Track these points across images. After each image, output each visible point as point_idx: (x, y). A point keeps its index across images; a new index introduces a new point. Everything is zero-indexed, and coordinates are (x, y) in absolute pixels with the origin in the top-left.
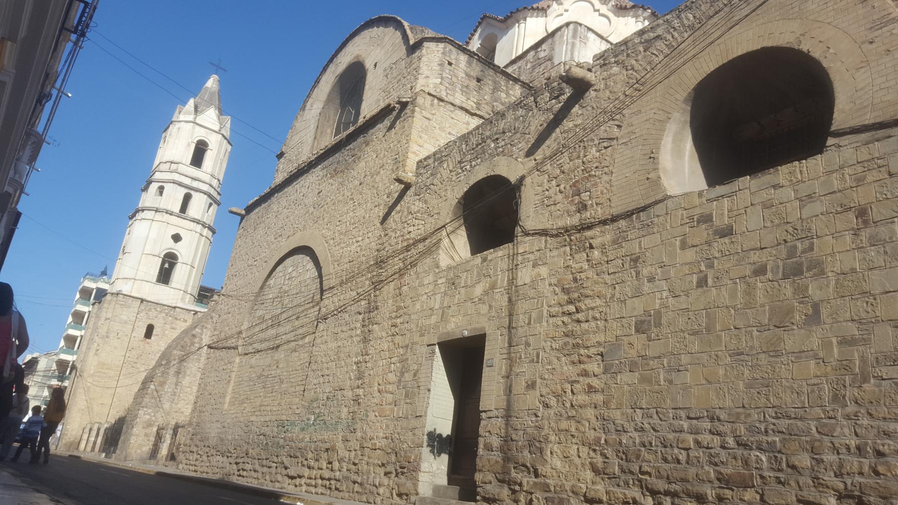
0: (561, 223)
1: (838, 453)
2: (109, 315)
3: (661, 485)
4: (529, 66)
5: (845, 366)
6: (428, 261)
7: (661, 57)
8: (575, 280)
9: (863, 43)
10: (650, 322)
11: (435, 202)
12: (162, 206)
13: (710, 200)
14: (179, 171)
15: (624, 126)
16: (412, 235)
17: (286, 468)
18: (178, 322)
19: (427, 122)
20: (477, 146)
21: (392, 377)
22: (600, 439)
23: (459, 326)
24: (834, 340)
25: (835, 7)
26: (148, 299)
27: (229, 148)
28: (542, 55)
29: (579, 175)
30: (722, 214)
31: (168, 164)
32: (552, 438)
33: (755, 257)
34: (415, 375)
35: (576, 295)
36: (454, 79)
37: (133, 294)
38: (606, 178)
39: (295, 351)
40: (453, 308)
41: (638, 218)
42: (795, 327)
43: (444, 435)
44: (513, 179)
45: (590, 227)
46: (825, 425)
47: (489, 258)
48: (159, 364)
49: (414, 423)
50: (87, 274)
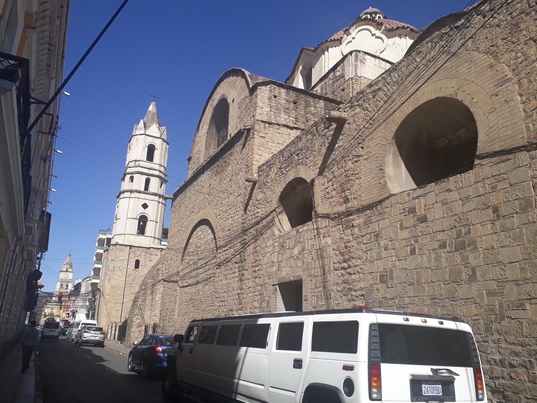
0: (336, 210)
1: (491, 365)
5: (491, 309)
6: (269, 232)
7: (382, 103)
8: (346, 247)
9: (492, 95)
10: (387, 276)
11: (269, 193)
12: (134, 188)
15: (365, 147)
16: (259, 214)
18: (153, 256)
19: (262, 140)
20: (288, 158)
21: (256, 304)
23: (287, 274)
24: (484, 292)
25: (476, 70)
27: (168, 147)
28: (338, 74)
29: (343, 179)
30: (421, 208)
31: (134, 162)
33: (440, 236)
34: (268, 304)
35: (347, 257)
38: (357, 181)
39: (206, 284)
40: (284, 262)
41: (377, 208)
42: (463, 283)
44: (308, 181)
45: (351, 214)
46: (482, 346)
47: (300, 231)
48: (141, 289)
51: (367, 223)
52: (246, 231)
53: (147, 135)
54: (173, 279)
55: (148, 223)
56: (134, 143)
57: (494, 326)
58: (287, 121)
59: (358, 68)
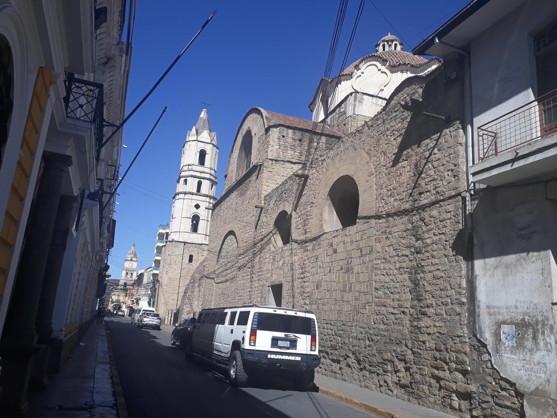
2: (170, 253)
6: (268, 247)
11: (269, 218)
12: (188, 190)
13: (334, 237)
14: (193, 169)
19: (270, 174)
21: (259, 299)
23: (275, 279)
27: (218, 151)
28: (342, 110)
29: (304, 217)
36: (286, 144)
38: (311, 220)
39: (232, 283)
40: (274, 270)
45: (306, 243)
51: (313, 249)
52: (256, 244)
53: (199, 141)
54: (211, 276)
55: (200, 221)
57: (355, 317)
58: (293, 156)
59: (356, 108)
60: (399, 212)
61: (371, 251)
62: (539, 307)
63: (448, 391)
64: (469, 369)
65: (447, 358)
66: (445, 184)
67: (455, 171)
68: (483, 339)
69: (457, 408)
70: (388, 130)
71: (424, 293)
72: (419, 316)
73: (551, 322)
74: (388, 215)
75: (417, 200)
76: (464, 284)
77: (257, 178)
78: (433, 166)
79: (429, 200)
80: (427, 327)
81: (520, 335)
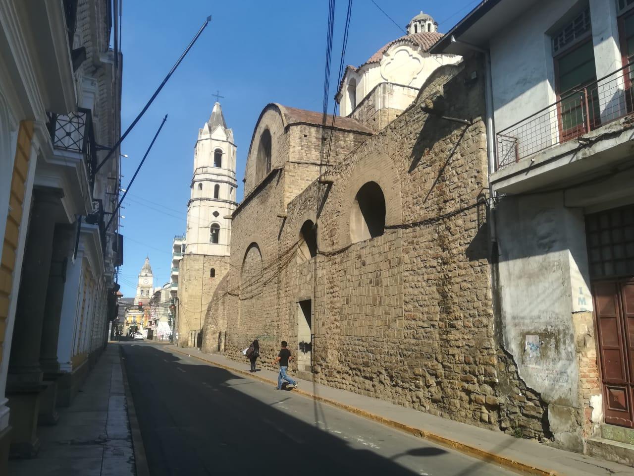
2: (188, 267)
3: (353, 366)
4: (366, 109)
11: (294, 229)
12: (204, 196)
13: (361, 249)
16: (288, 245)
17: (261, 358)
19: (293, 178)
21: (287, 317)
22: (339, 347)
23: (304, 294)
26: (208, 254)
27: (236, 149)
28: (371, 103)
31: (201, 169)
32: (329, 347)
33: (370, 276)
35: (332, 285)
36: (310, 144)
37: (198, 253)
38: (338, 231)
39: (258, 299)
43: (308, 343)
45: (334, 254)
49: (295, 339)
50: (176, 236)
51: (342, 262)
56: (200, 148)
57: (386, 332)
59: (386, 100)
60: (425, 221)
61: (399, 263)
62: (560, 317)
63: (478, 403)
64: (497, 381)
65: (477, 371)
66: (469, 191)
67: (477, 179)
68: (510, 350)
69: (487, 420)
70: (411, 133)
71: (452, 305)
72: (448, 329)
73: (571, 332)
74: (415, 224)
75: (442, 209)
76: (490, 295)
77: (277, 184)
78: (457, 173)
79: (454, 208)
80: (457, 340)
81: (543, 345)
